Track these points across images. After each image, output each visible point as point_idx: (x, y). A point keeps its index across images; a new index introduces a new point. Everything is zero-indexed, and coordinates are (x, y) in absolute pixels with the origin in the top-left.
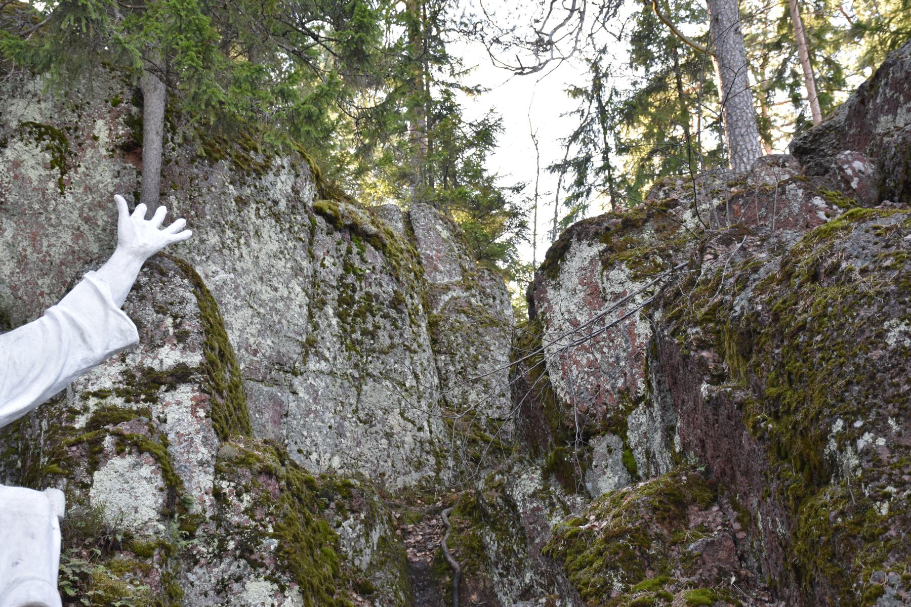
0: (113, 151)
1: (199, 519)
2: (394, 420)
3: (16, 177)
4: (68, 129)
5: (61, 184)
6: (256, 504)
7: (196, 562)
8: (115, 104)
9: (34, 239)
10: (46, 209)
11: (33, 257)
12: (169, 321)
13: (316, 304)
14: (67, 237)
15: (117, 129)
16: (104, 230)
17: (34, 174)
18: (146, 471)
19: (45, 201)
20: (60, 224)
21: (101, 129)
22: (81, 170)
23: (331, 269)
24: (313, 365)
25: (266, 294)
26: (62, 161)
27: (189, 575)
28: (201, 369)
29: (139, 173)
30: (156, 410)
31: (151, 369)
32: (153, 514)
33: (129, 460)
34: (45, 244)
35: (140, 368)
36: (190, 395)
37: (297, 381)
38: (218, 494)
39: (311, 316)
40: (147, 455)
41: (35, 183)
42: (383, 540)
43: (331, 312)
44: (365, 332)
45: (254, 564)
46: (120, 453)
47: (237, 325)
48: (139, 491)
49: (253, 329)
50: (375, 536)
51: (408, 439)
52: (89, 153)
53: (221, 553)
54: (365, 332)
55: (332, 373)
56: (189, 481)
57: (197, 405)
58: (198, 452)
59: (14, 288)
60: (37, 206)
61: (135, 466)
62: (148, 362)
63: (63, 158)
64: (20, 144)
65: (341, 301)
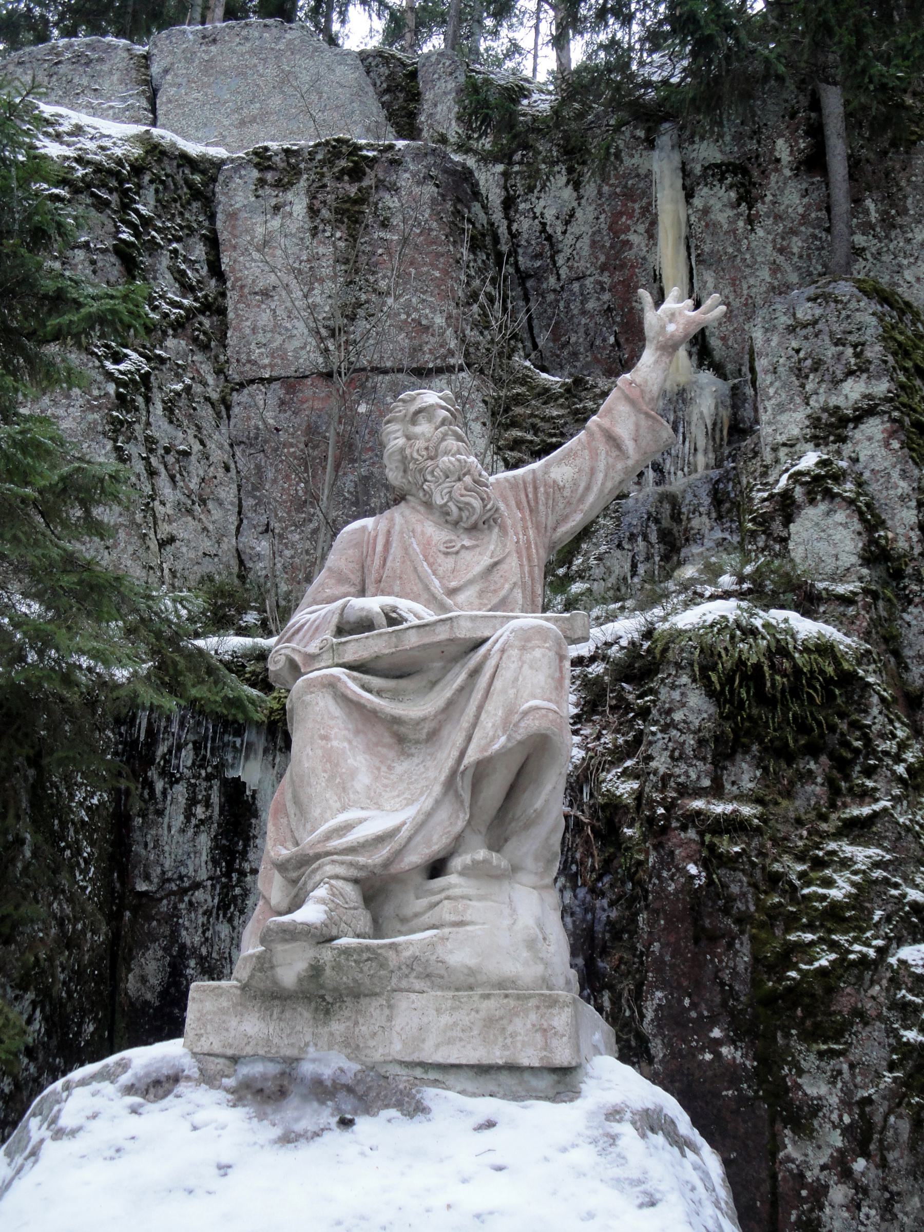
0: (797, 168)
3: (707, 225)
4: (749, 159)
5: (750, 221)
7: (910, 602)
8: (793, 116)
9: (734, 285)
10: (739, 250)
12: (850, 351)
14: (765, 274)
15: (797, 143)
16: (801, 257)
17: (722, 216)
18: (840, 516)
19: (737, 242)
20: (756, 262)
21: (782, 148)
22: (769, 198)
26: (747, 196)
27: (905, 615)
29: (827, 186)
30: (847, 449)
31: (837, 408)
32: (854, 559)
33: (823, 507)
34: (745, 286)
36: (881, 427)
40: (838, 500)
41: (725, 226)
46: (812, 501)
48: (837, 537)
52: (773, 177)
56: (892, 519)
57: (890, 436)
58: (897, 487)
59: (724, 339)
60: (730, 250)
61: (828, 513)
62: (834, 401)
63: (748, 192)
64: (706, 190)
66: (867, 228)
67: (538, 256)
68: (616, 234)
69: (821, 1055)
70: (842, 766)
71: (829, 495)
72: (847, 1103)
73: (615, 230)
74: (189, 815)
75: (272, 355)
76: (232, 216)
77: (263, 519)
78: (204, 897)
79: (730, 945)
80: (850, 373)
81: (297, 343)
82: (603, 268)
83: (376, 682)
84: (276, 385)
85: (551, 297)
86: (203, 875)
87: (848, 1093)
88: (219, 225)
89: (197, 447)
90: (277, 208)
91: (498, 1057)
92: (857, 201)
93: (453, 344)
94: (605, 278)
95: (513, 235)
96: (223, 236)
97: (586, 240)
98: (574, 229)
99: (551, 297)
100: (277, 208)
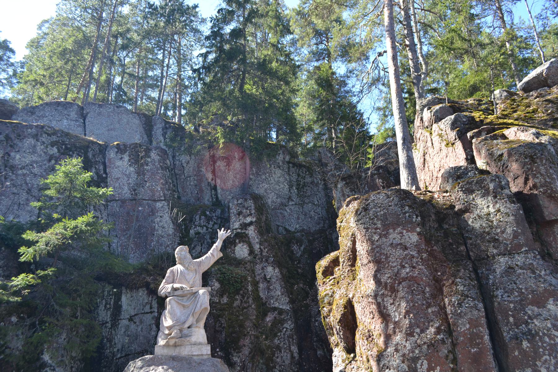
1: (257, 255)
2: (312, 213)
6: (268, 250)
11: (224, 188)
13: (291, 187)
14: (231, 182)
18: (245, 246)
23: (294, 177)
24: (290, 203)
25: (278, 187)
26: (228, 164)
28: (256, 221)
35: (243, 223)
37: (286, 208)
38: (260, 248)
39: (290, 190)
42: (304, 248)
43: (295, 188)
44: (303, 192)
45: (268, 263)
46: (240, 243)
47: (271, 197)
49: (275, 197)
50: (302, 248)
51: (316, 218)
53: (262, 262)
54: (303, 192)
55: (296, 204)
59: (222, 195)
62: (245, 221)
65: (297, 185)
66: (253, 174)
67: (180, 170)
68: (199, 168)
69: (237, 353)
70: (243, 297)
71: (243, 242)
72: (241, 362)
73: (199, 167)
74: (105, 306)
75: (119, 194)
76: (110, 160)
77: (115, 234)
78: (109, 325)
79: (221, 333)
80: (249, 215)
81: (124, 192)
82: (195, 175)
83: (180, 298)
84: (119, 202)
85: (182, 180)
86: (109, 320)
87: (241, 359)
88: (106, 161)
89: (100, 216)
90: (121, 158)
91: (200, 353)
92: (251, 168)
93: (162, 194)
94: (196, 178)
95: (174, 165)
96: (107, 164)
97: (191, 169)
98: (189, 165)
99: (182, 180)
100: (121, 158)
